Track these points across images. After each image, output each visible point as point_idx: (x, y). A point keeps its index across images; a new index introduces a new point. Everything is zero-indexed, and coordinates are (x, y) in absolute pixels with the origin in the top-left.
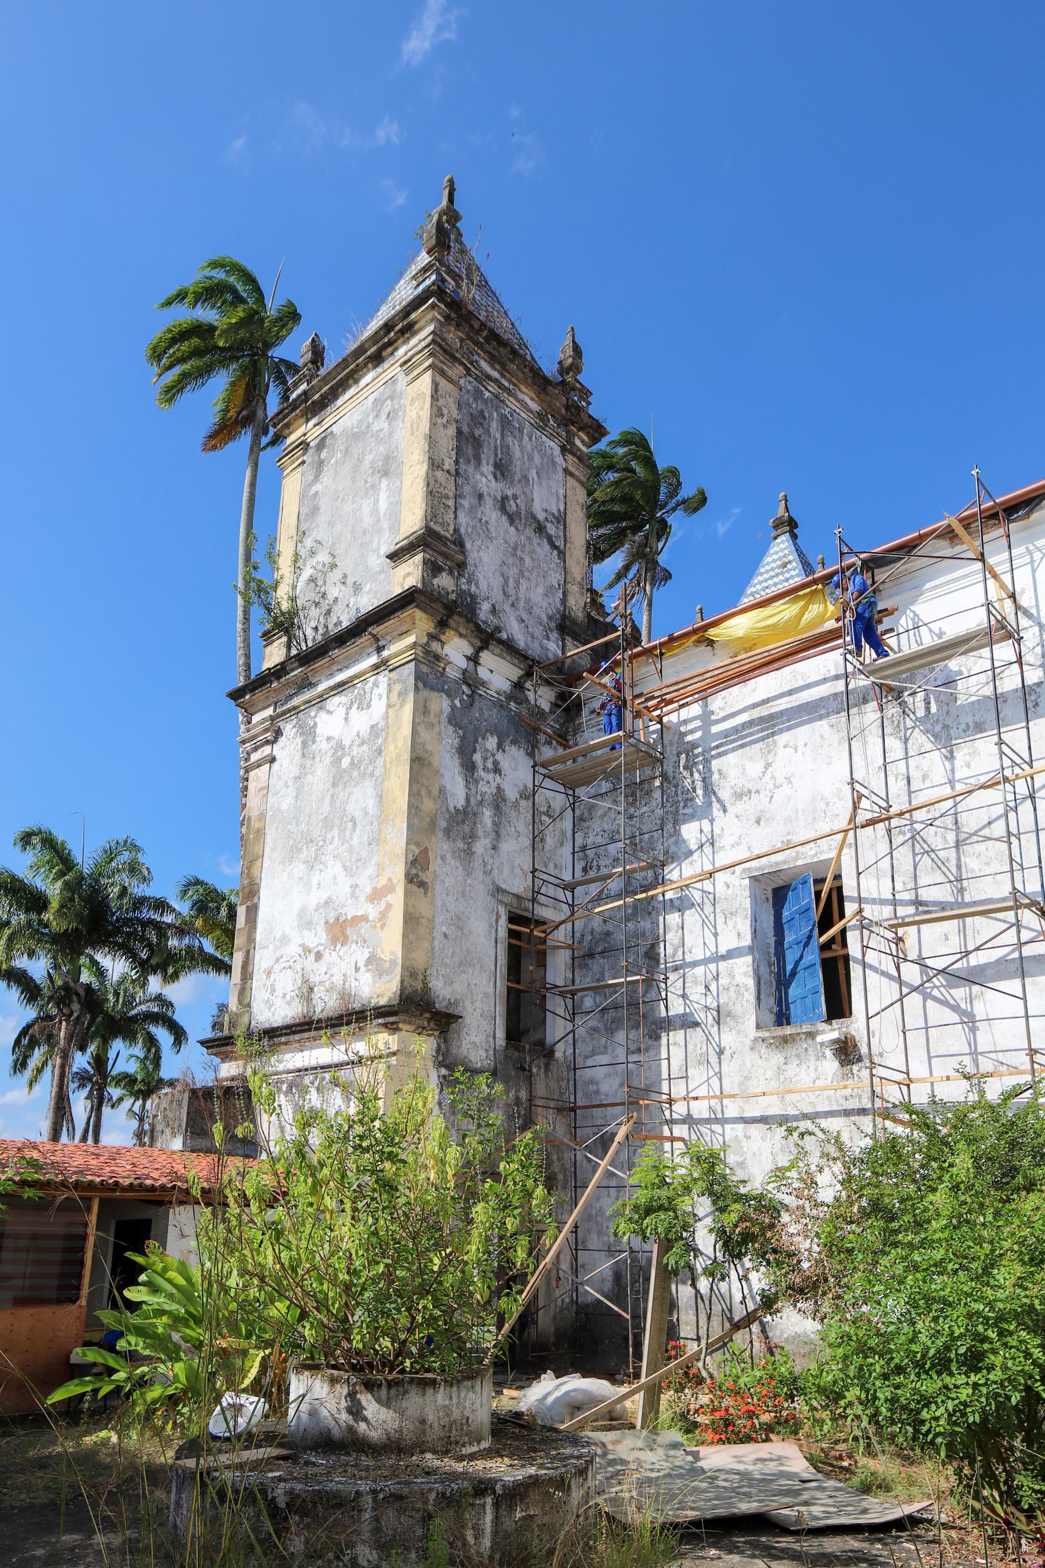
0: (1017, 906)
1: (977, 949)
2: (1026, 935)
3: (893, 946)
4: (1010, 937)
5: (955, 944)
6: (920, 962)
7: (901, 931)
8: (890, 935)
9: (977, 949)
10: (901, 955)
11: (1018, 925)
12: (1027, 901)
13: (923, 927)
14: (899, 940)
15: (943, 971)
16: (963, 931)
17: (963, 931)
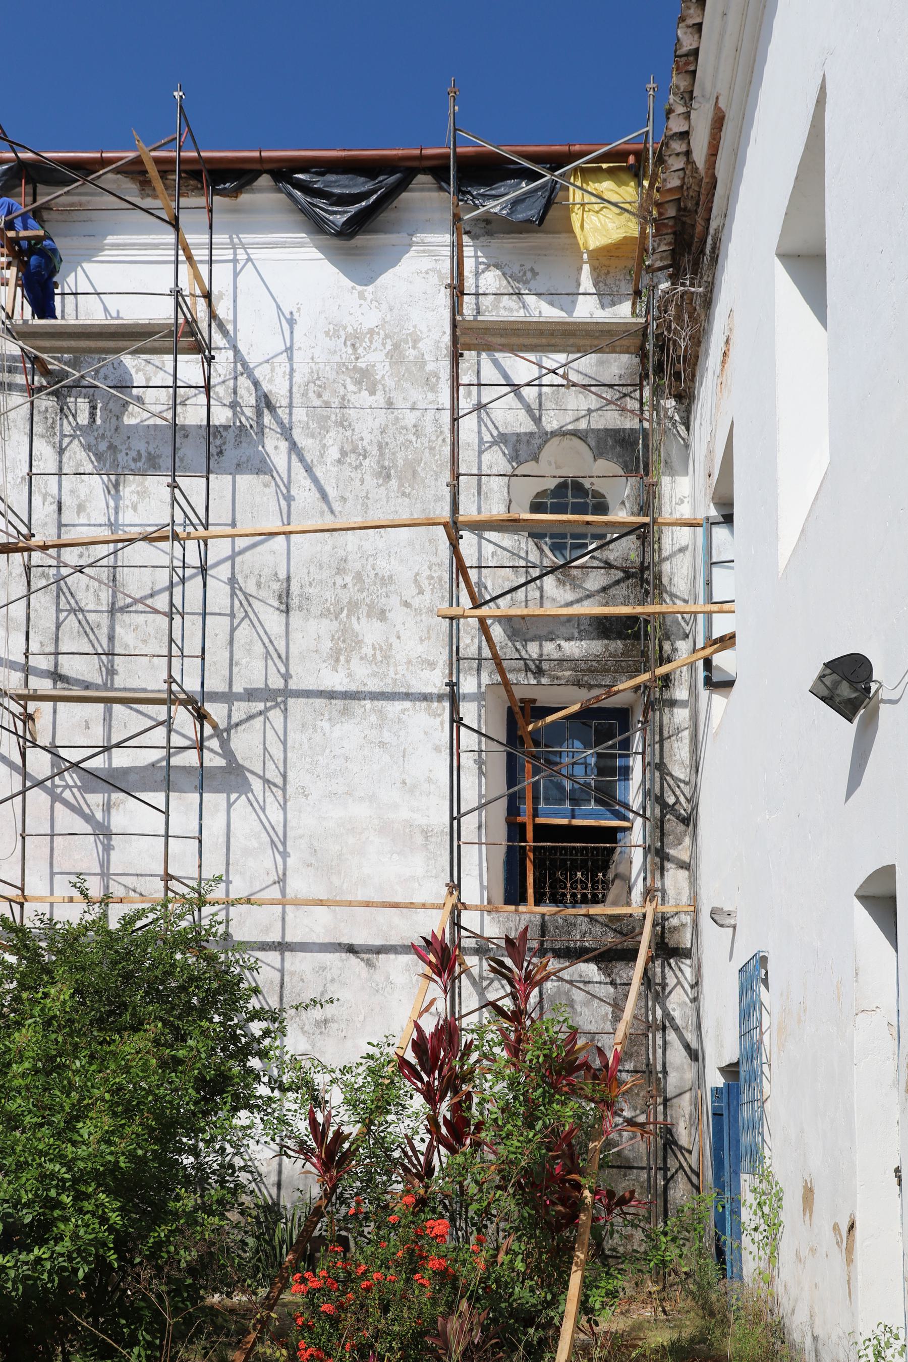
0: (170, 700)
1: (118, 746)
2: (176, 740)
3: (20, 724)
4: (158, 736)
5: (97, 737)
6: (52, 749)
7: (32, 706)
8: (17, 709)
9: (118, 746)
10: (28, 737)
11: (168, 723)
12: (183, 696)
13: (60, 705)
14: (28, 718)
15: (76, 765)
16: (108, 719)
17: (108, 719)
